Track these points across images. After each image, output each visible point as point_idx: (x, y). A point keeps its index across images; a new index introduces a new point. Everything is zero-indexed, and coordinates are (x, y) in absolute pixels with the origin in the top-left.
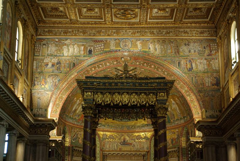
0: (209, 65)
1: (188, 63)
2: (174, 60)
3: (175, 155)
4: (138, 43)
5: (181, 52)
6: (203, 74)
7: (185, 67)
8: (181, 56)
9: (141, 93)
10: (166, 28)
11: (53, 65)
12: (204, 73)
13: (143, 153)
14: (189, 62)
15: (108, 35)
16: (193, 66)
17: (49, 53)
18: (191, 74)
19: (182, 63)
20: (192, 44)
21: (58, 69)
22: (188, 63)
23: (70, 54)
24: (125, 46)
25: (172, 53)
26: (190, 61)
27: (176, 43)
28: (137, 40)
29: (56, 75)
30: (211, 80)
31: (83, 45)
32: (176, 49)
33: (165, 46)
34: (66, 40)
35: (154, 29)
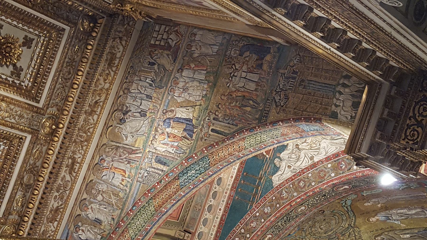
1: (169, 130)
2: (146, 174)
5: (136, 141)
6: (217, 92)
7: (176, 144)
12: (215, 85)
14: (169, 127)
16: (184, 116)
18: (201, 130)
22: (169, 130)
25: (124, 171)
27: (107, 150)
30: (245, 68)
32: (120, 156)
33: (100, 187)
35: (46, 205)
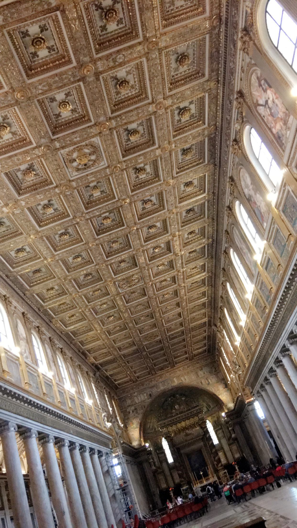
0: (218, 377)
3: (220, 431)
4: (175, 379)
8: (201, 378)
9: (190, 418)
10: (186, 365)
11: (133, 412)
13: (201, 437)
15: (157, 381)
17: (128, 405)
19: (203, 382)
20: (204, 369)
21: (137, 413)
23: (140, 401)
24: (168, 384)
26: (207, 379)
28: (173, 378)
29: (136, 417)
31: (145, 393)
34: (134, 393)
